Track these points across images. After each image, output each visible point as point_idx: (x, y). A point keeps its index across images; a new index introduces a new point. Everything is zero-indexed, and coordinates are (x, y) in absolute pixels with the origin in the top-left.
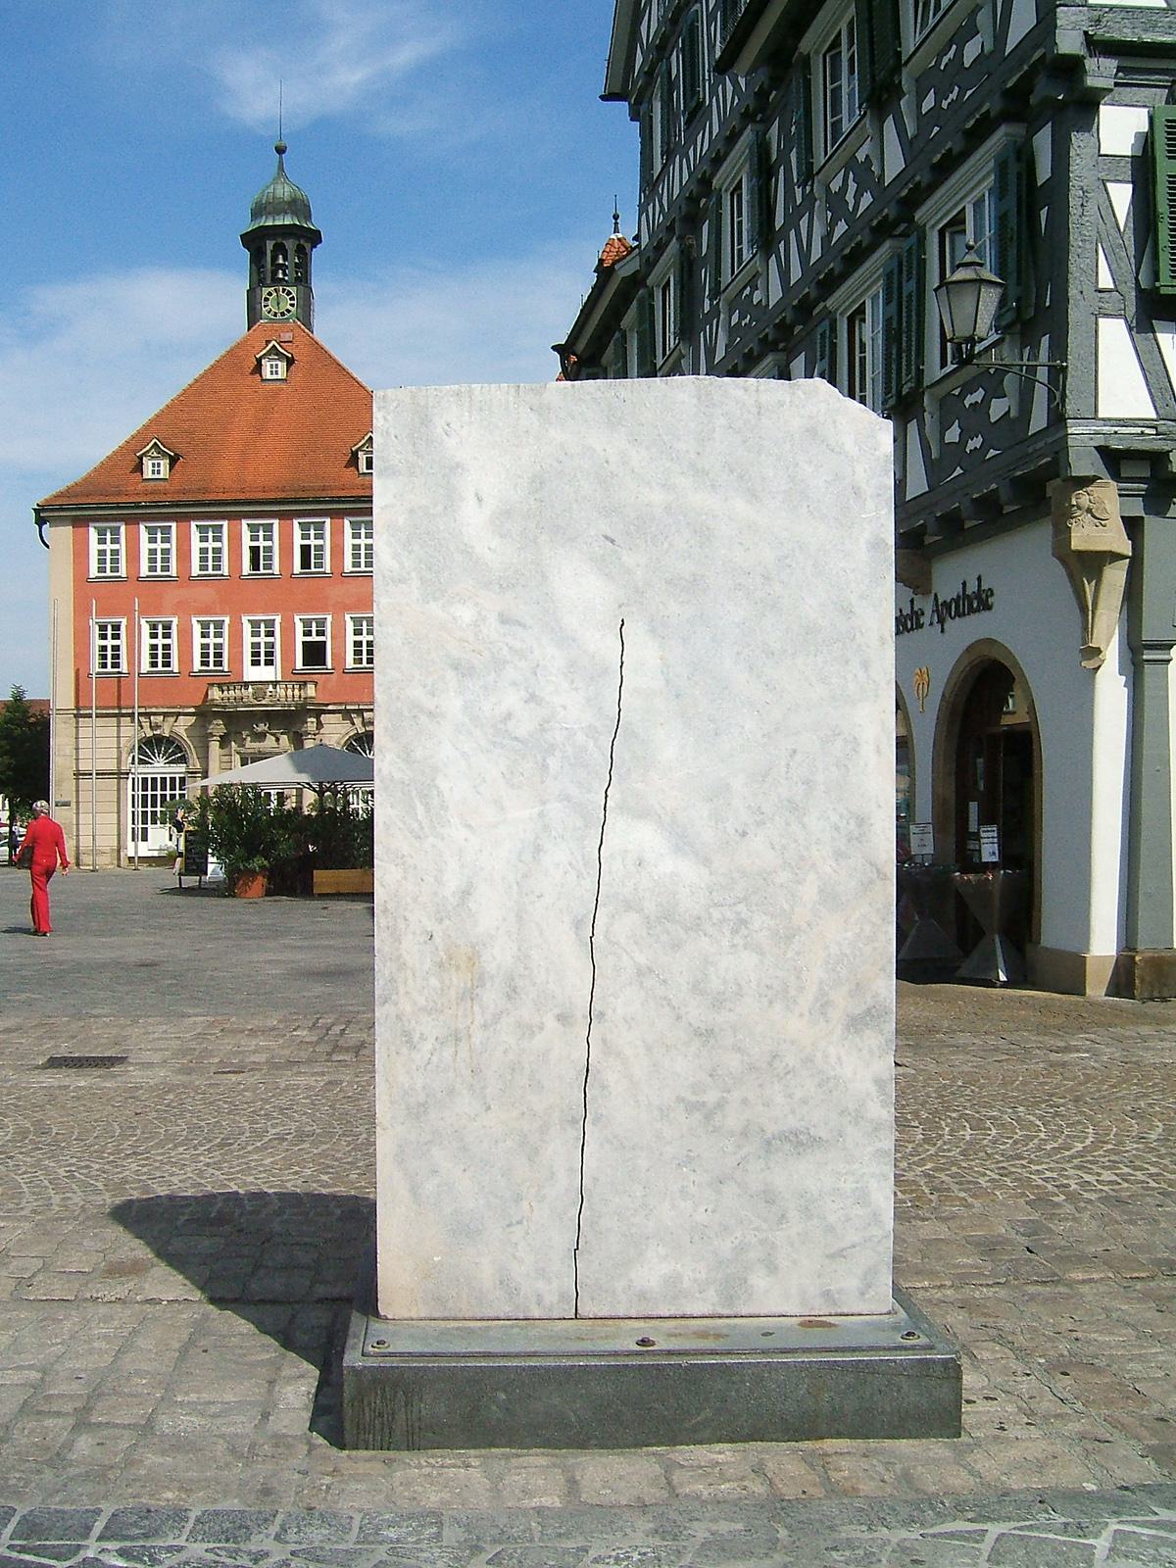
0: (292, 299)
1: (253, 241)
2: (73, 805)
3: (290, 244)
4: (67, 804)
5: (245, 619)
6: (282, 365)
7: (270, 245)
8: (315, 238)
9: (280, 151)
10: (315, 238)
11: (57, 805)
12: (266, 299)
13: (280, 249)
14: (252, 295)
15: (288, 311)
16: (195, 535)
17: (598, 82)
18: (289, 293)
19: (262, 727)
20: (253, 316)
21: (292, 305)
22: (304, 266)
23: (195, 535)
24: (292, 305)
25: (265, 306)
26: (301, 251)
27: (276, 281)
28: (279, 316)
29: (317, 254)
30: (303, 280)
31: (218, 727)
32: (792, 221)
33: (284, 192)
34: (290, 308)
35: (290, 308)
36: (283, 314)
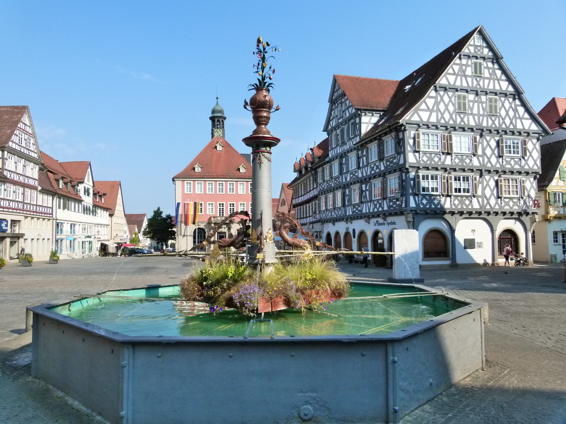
1: (212, 119)
3: (221, 120)
5: (208, 203)
6: (221, 147)
7: (216, 120)
8: (225, 118)
9: (217, 98)
10: (225, 118)
13: (218, 121)
14: (212, 131)
16: (207, 184)
17: (322, 128)
20: (213, 136)
22: (223, 124)
23: (207, 184)
26: (223, 121)
27: (218, 128)
29: (225, 122)
30: (223, 127)
32: (333, 119)
33: (218, 108)
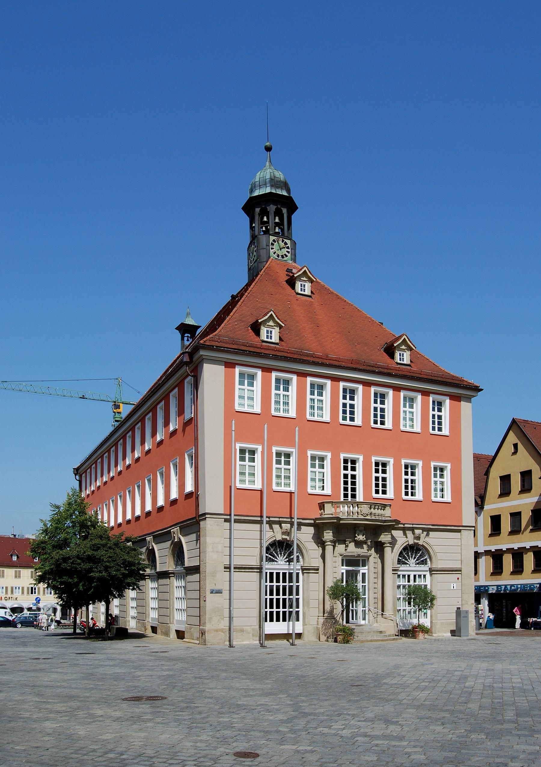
0: (288, 248)
2: (226, 594)
4: (219, 592)
11: (212, 593)
12: (272, 244)
15: (287, 256)
18: (286, 244)
19: (361, 537)
21: (288, 252)
24: (288, 252)
25: (272, 249)
28: (280, 258)
31: (328, 535)
34: (287, 254)
35: (287, 254)
36: (283, 257)
